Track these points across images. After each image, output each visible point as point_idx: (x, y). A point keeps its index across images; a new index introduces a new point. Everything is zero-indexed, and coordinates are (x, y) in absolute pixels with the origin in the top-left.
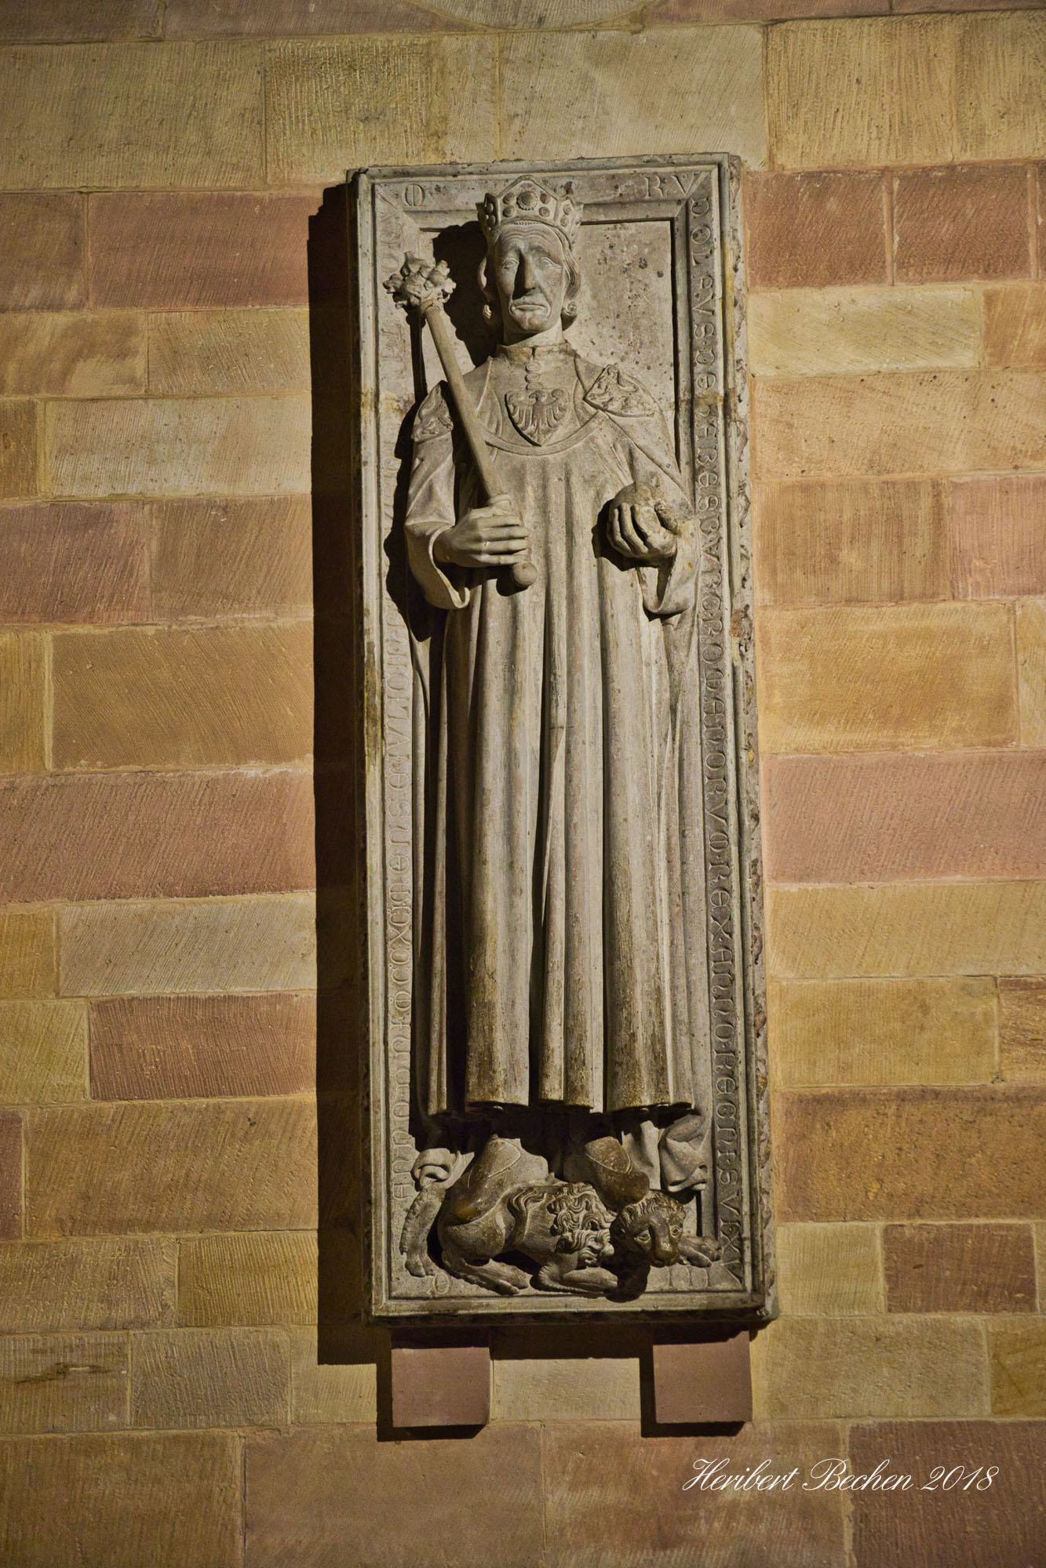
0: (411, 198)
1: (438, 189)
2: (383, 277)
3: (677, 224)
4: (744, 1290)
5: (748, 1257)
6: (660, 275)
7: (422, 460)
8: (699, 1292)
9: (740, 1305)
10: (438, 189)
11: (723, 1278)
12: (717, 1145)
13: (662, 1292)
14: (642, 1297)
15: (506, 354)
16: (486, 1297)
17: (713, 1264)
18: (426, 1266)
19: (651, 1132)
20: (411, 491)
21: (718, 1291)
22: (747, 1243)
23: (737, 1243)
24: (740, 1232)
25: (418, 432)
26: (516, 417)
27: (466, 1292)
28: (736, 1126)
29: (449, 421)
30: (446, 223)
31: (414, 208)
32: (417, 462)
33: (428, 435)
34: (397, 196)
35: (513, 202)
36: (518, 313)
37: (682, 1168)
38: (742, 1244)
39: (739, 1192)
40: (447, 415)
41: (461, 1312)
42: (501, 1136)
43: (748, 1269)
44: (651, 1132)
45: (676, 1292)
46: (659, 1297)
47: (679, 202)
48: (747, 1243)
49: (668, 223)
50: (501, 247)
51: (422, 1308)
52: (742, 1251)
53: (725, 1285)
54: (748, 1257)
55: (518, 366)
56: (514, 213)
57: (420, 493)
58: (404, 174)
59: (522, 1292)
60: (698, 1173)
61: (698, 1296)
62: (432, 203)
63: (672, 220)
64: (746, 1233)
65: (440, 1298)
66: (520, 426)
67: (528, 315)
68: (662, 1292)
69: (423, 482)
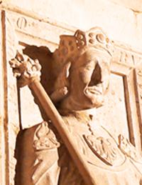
0: (19, 24)
1: (33, 24)
2: (8, 59)
3: (130, 80)
6: (121, 100)
7: (41, 161)
10: (33, 24)
15: (75, 115)
20: (34, 178)
25: (38, 144)
26: (94, 147)
29: (56, 142)
30: (31, 42)
31: (19, 29)
32: (37, 162)
33: (44, 147)
34: (14, 20)
35: (94, 37)
36: (89, 94)
40: (55, 138)
47: (131, 68)
49: (121, 78)
50: (85, 60)
55: (83, 122)
56: (96, 42)
57: (40, 179)
58: (19, 12)
62: (29, 30)
63: (124, 77)
66: (99, 152)
67: (95, 96)
69: (42, 174)
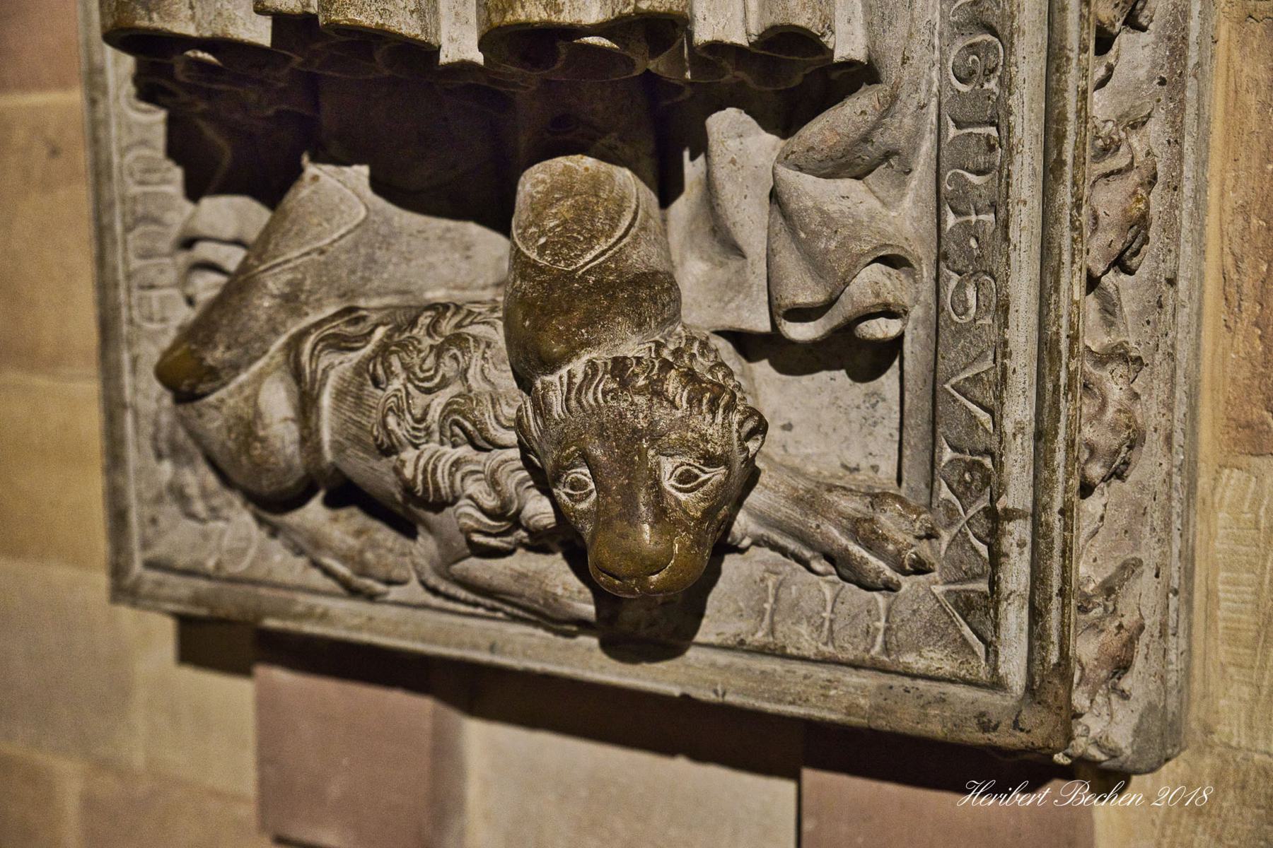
4: (997, 684)
5: (1016, 575)
8: (856, 666)
9: (972, 735)
11: (931, 631)
12: (947, 187)
13: (740, 647)
14: (691, 653)
16: (315, 592)
17: (907, 583)
18: (205, 494)
19: (739, 141)
21: (908, 674)
22: (1018, 530)
23: (983, 526)
24: (992, 482)
27: (281, 575)
28: (998, 117)
37: (816, 264)
38: (993, 537)
39: (1003, 349)
41: (272, 623)
42: (315, 159)
43: (1014, 618)
44: (739, 141)
45: (780, 653)
46: (740, 661)
48: (1018, 530)
51: (197, 600)
52: (996, 557)
53: (935, 659)
54: (1016, 575)
59: (395, 593)
60: (870, 282)
61: (853, 678)
64: (1017, 495)
65: (233, 580)
68: (740, 647)
